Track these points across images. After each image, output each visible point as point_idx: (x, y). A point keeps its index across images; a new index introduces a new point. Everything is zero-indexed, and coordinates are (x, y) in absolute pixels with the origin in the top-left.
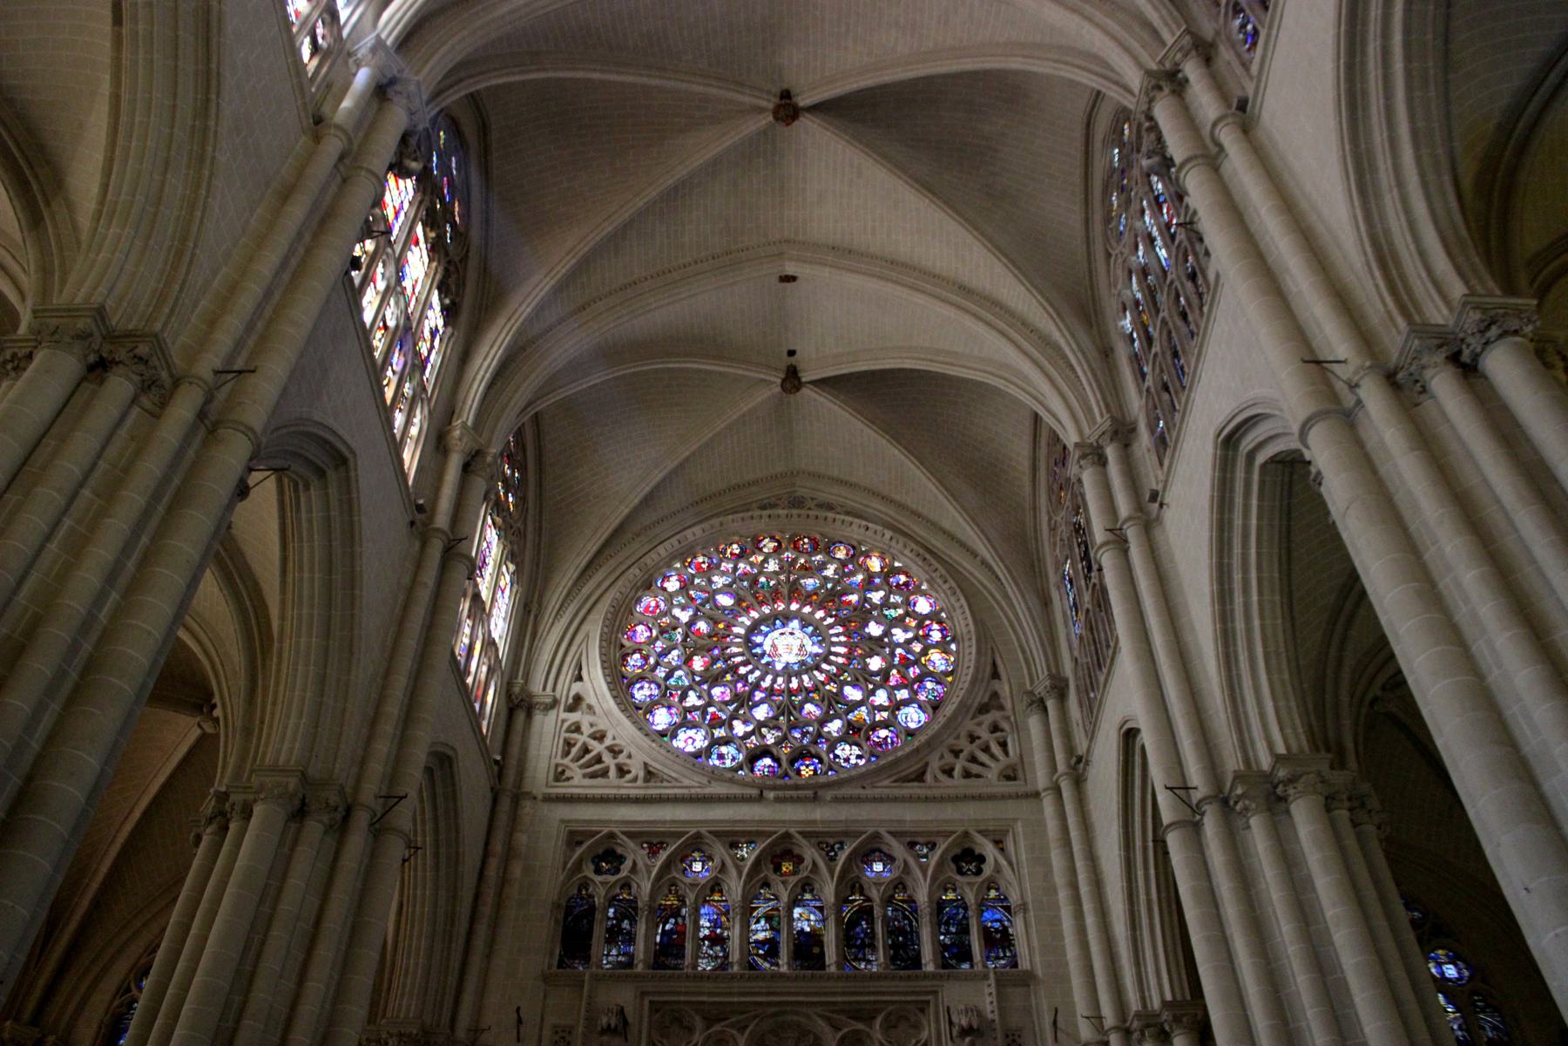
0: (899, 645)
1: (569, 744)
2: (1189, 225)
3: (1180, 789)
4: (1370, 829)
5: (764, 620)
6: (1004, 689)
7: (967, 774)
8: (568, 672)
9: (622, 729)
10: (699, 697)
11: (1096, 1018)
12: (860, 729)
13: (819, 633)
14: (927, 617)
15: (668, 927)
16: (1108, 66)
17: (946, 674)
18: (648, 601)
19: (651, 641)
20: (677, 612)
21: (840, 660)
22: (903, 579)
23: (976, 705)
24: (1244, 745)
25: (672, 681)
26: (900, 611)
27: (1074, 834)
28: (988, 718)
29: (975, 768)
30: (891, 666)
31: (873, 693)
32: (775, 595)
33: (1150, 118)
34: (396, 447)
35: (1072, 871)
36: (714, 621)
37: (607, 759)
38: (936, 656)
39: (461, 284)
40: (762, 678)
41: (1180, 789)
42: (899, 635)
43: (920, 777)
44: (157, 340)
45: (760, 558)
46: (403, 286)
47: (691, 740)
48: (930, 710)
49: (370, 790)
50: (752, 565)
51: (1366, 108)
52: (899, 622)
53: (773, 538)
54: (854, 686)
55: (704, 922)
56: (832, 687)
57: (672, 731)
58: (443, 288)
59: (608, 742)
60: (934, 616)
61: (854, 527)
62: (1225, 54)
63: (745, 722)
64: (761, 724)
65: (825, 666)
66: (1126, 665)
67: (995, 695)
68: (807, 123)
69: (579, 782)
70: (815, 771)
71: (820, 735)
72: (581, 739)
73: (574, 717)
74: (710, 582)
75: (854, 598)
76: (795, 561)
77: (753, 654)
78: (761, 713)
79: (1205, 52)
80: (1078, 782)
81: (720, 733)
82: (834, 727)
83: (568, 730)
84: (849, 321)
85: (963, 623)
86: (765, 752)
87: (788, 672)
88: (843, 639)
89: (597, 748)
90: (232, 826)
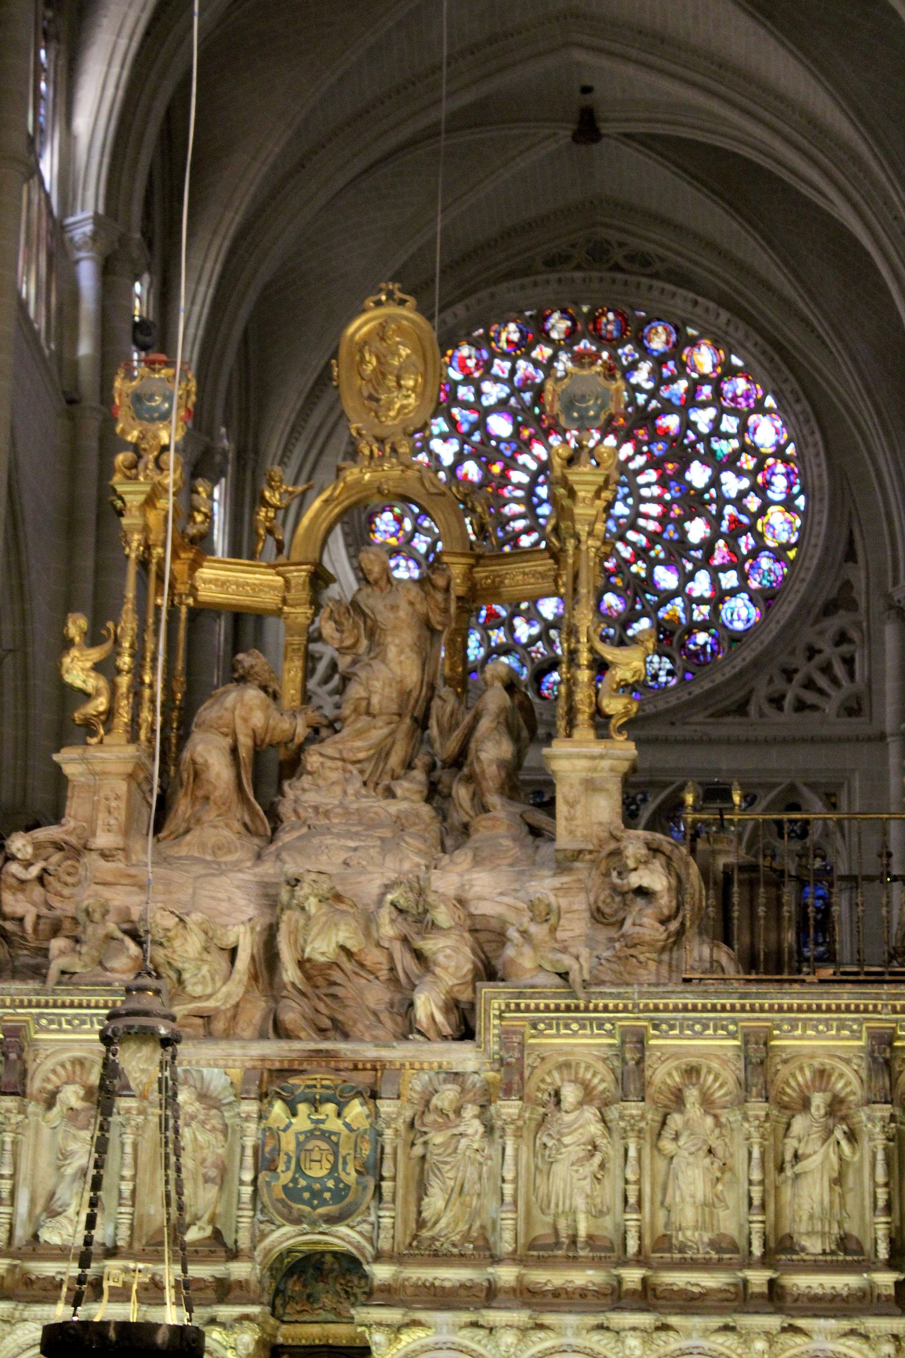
0: (729, 501)
7: (801, 706)
12: (672, 633)
21: (652, 526)
23: (820, 603)
28: (833, 624)
29: (810, 697)
30: (717, 534)
31: (691, 577)
38: (776, 516)
42: (732, 484)
43: (742, 709)
45: (548, 352)
48: (762, 603)
52: (731, 462)
53: (564, 311)
56: (639, 568)
60: (779, 452)
61: (679, 301)
63: (528, 622)
64: (548, 626)
65: (631, 535)
67: (847, 585)
74: (479, 393)
75: (671, 422)
81: (498, 636)
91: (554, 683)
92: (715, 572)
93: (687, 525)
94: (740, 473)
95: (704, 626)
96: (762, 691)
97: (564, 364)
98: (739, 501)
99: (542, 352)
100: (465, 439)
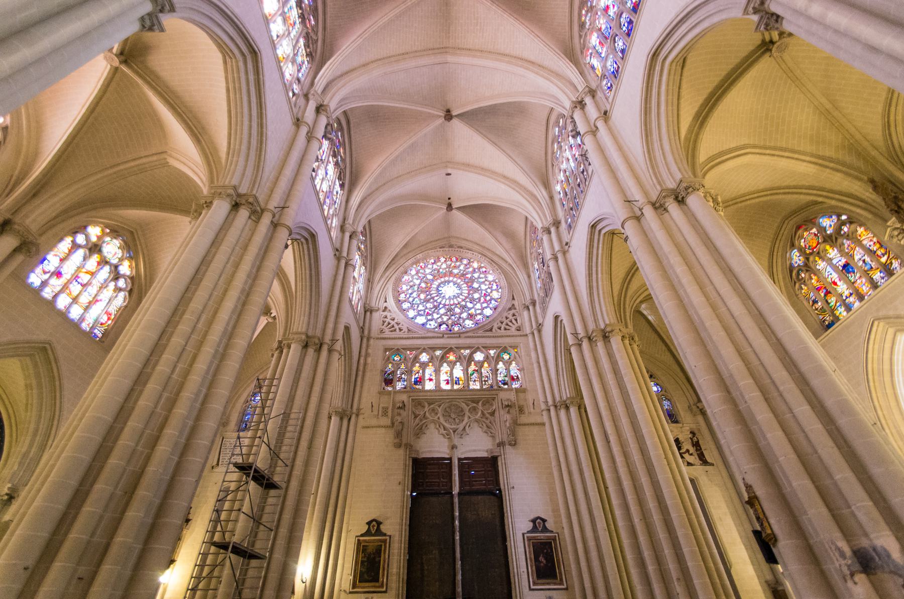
1: (384, 322)
2: (584, 155)
3: (575, 334)
4: (635, 346)
5: (442, 283)
6: (516, 303)
7: (505, 329)
8: (383, 300)
9: (399, 317)
11: (546, 402)
13: (459, 287)
16: (558, 100)
18: (406, 277)
19: (408, 290)
20: (415, 281)
22: (484, 269)
24: (596, 321)
27: (539, 347)
29: (507, 327)
32: (445, 275)
33: (572, 118)
34: (329, 230)
35: (538, 358)
37: (396, 327)
39: (344, 176)
41: (575, 334)
42: (483, 287)
43: (491, 330)
44: (255, 197)
46: (326, 177)
47: (421, 320)
49: (328, 338)
51: (650, 113)
56: (463, 303)
58: (340, 179)
60: (494, 281)
62: (599, 94)
66: (556, 296)
68: (455, 122)
69: (388, 333)
72: (388, 320)
75: (469, 276)
77: (439, 293)
78: (442, 311)
79: (592, 93)
80: (539, 331)
81: (429, 317)
82: (464, 315)
84: (469, 187)
85: (504, 283)
87: (450, 298)
89: (393, 323)
90: (285, 351)
95: (480, 314)
96: (496, 326)
99: (439, 264)
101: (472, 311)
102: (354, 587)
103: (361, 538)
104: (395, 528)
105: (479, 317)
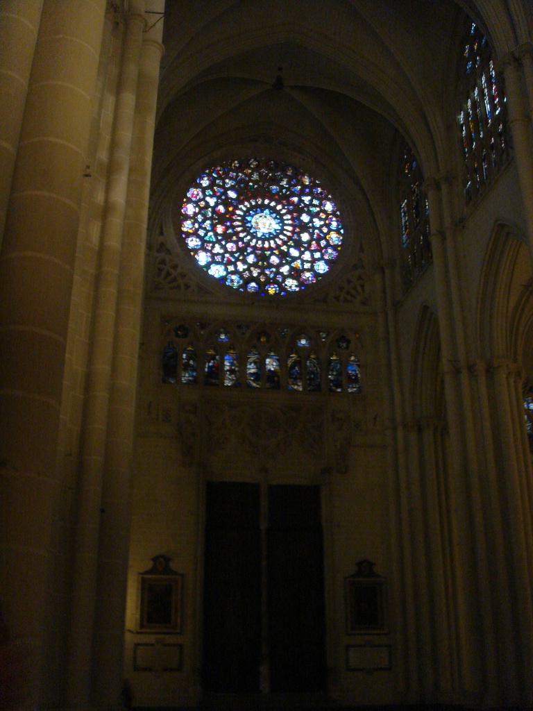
0: (317, 228)
7: (346, 301)
10: (221, 248)
14: (331, 214)
15: (211, 364)
17: (338, 246)
20: (208, 199)
21: (289, 234)
25: (207, 238)
26: (318, 209)
30: (312, 239)
36: (226, 206)
40: (251, 240)
42: (317, 223)
47: (217, 271)
50: (246, 175)
52: (317, 215)
53: (256, 160)
54: (295, 249)
55: (227, 363)
57: (208, 266)
59: (179, 270)
60: (334, 213)
64: (250, 265)
65: (281, 236)
70: (276, 291)
71: (278, 273)
73: (162, 255)
76: (267, 174)
81: (231, 268)
82: (285, 270)
83: (159, 263)
86: (252, 279)
87: (264, 239)
88: (290, 222)
91: (252, 287)
92: (312, 252)
93: (301, 235)
94: (321, 219)
97: (255, 176)
98: (320, 229)
100: (219, 198)
101: (298, 264)
102: (142, 626)
103: (145, 576)
104: (187, 564)
105: (308, 275)
